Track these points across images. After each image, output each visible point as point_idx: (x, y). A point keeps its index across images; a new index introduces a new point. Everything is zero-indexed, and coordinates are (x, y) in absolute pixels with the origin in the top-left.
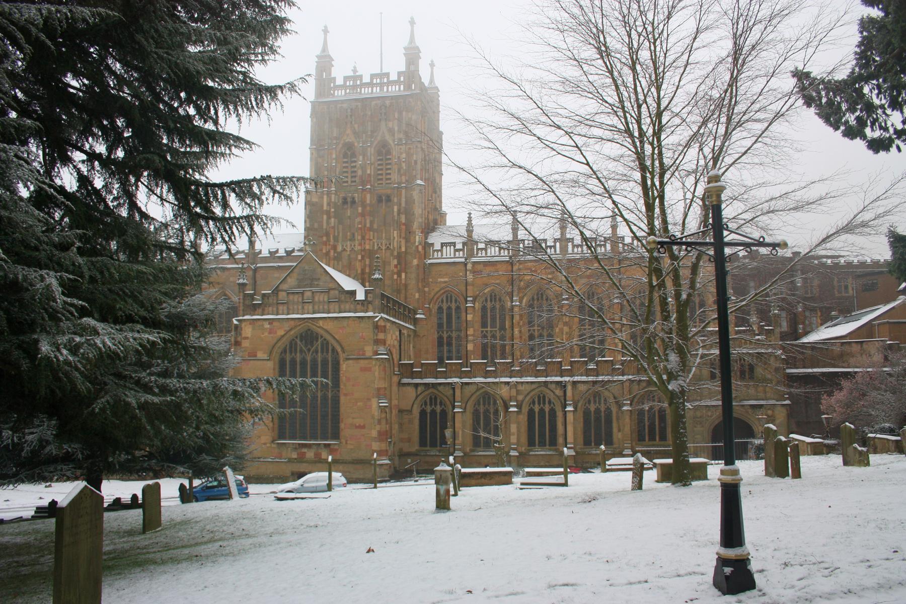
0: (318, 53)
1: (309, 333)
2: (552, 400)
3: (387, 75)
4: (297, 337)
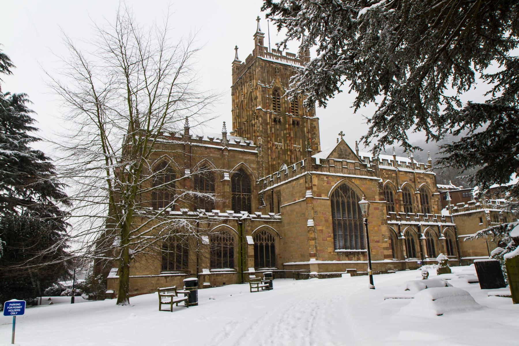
1: (344, 186)
2: (412, 234)
4: (338, 188)
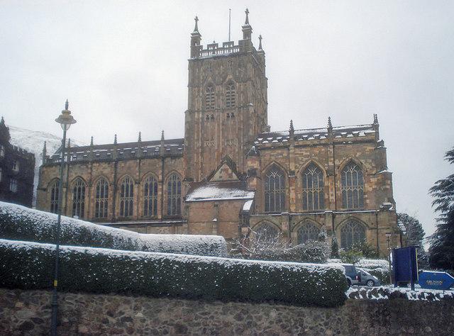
0: (192, 31)
3: (233, 43)
